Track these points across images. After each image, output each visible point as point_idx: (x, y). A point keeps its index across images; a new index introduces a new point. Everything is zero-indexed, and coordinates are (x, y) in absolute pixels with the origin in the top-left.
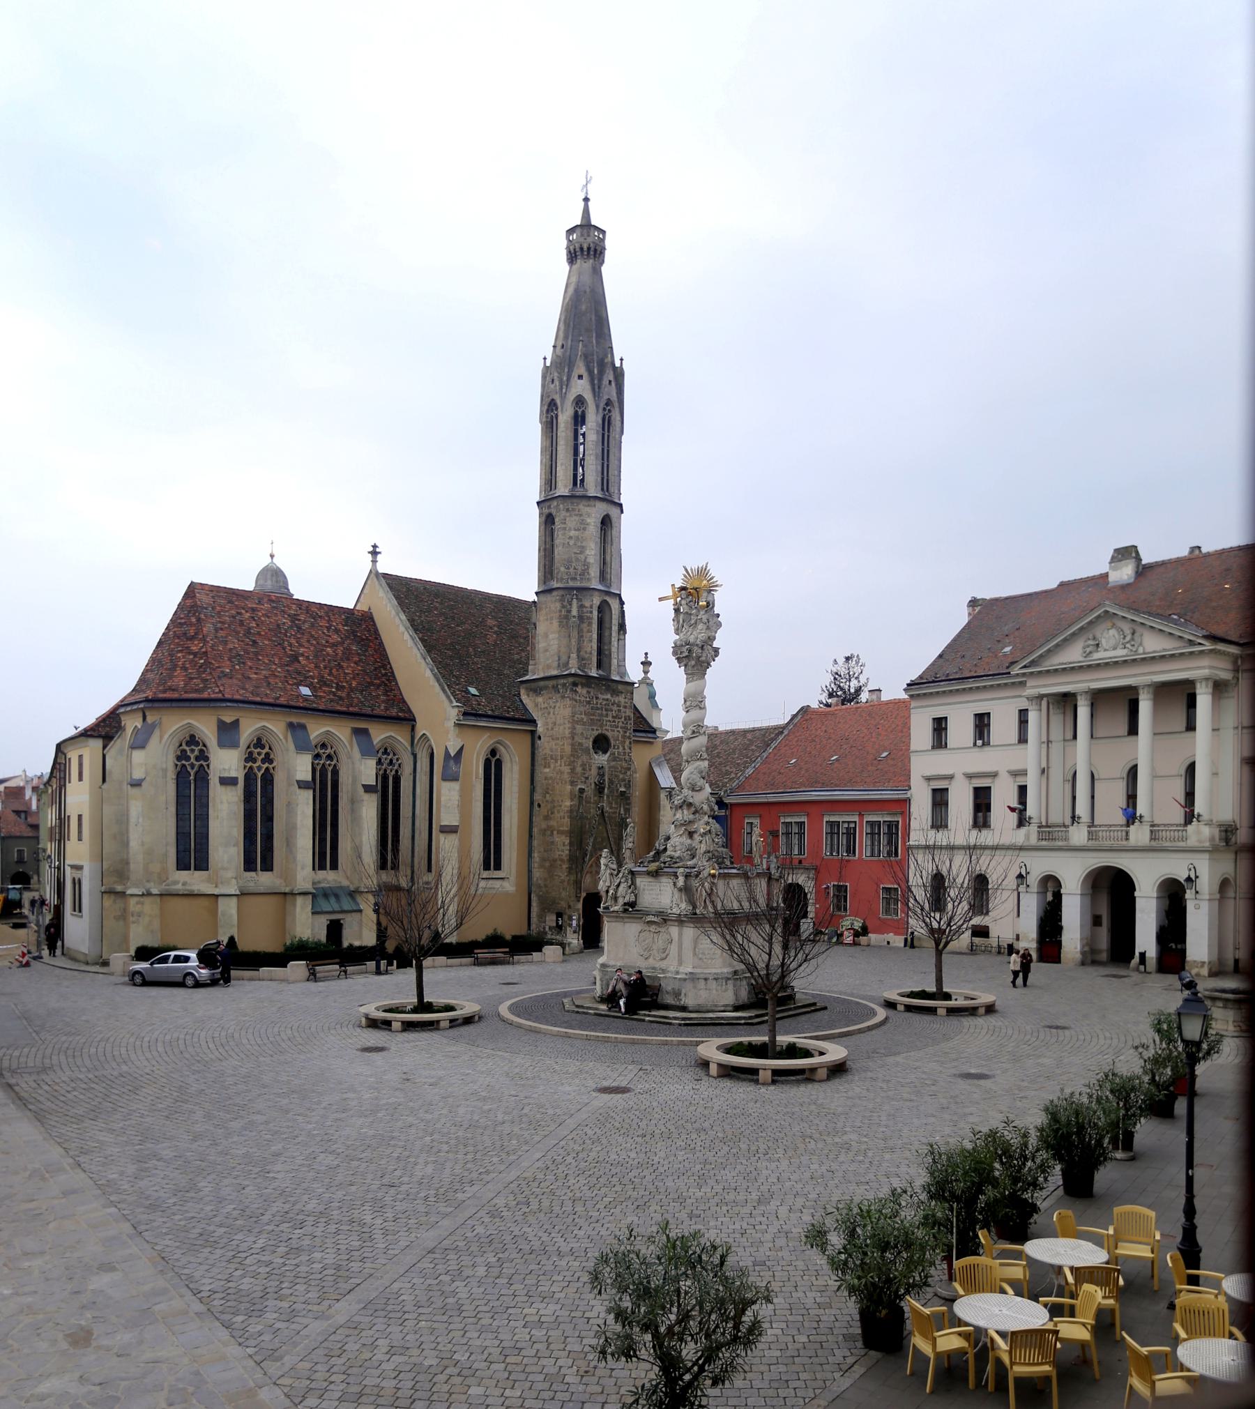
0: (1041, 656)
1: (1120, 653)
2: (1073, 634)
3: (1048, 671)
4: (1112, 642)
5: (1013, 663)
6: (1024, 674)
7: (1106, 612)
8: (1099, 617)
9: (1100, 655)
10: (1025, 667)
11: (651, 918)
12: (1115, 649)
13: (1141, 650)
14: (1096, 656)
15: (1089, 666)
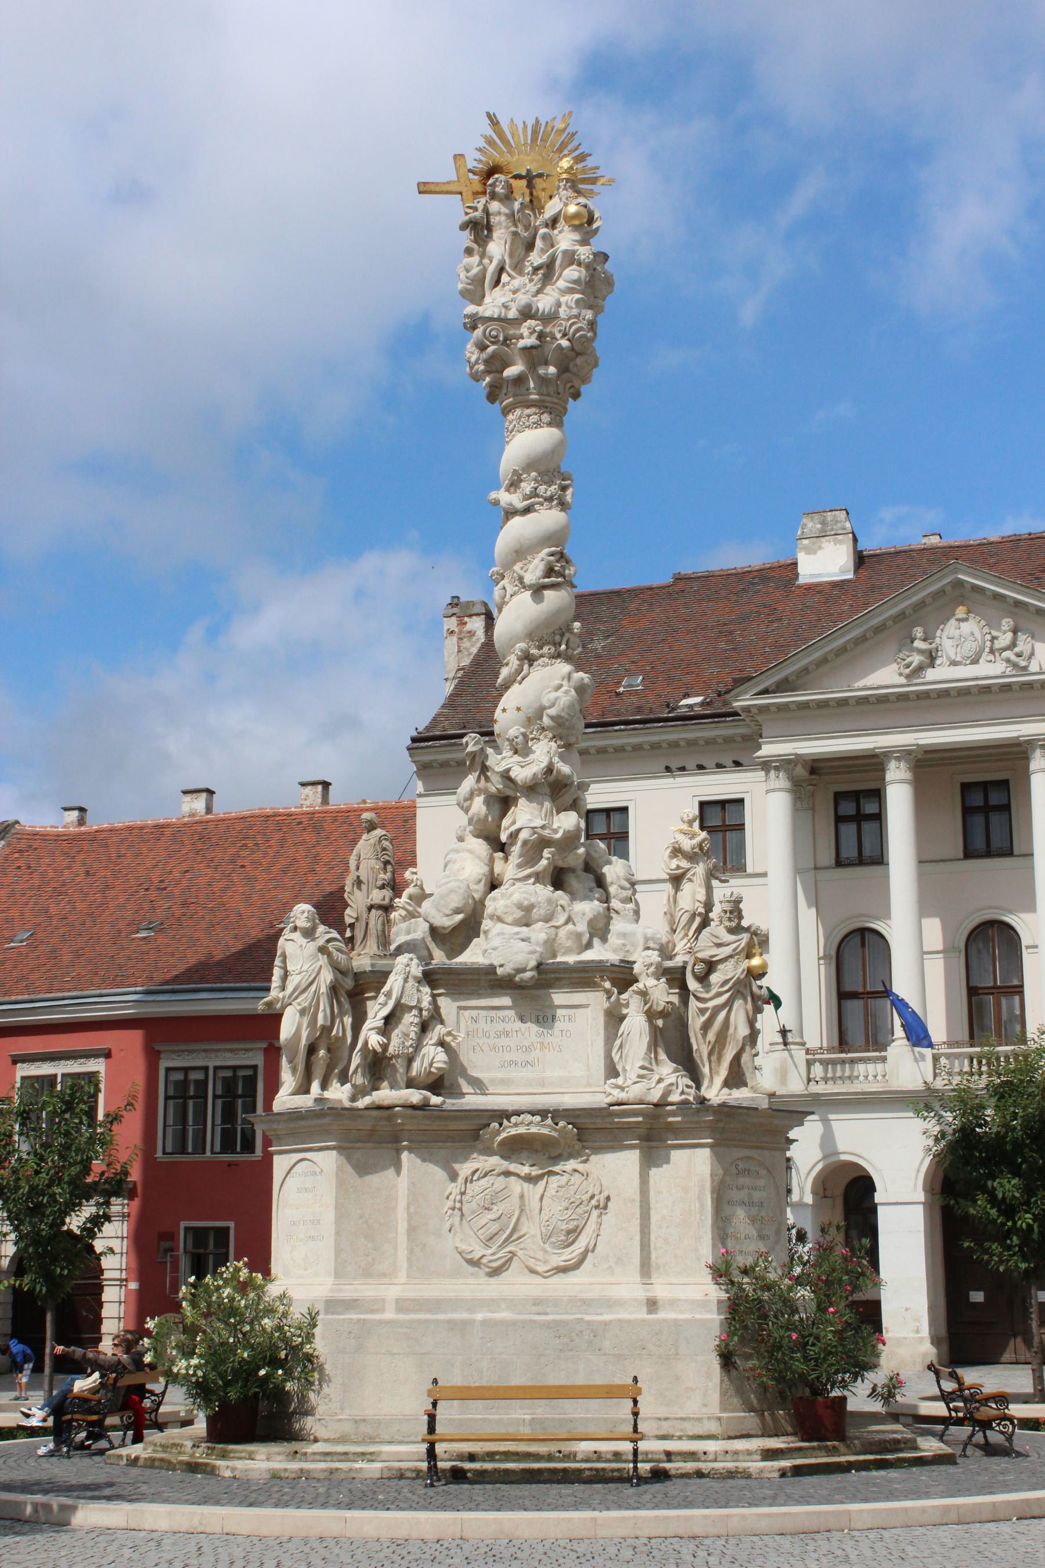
0: (806, 670)
1: (991, 670)
2: (879, 630)
3: (843, 702)
4: (969, 647)
5: (739, 682)
6: (763, 709)
7: (960, 583)
8: (942, 592)
9: (939, 675)
10: (765, 692)
11: (511, 1130)
12: (975, 661)
13: (1034, 667)
14: (931, 675)
15: (925, 695)
